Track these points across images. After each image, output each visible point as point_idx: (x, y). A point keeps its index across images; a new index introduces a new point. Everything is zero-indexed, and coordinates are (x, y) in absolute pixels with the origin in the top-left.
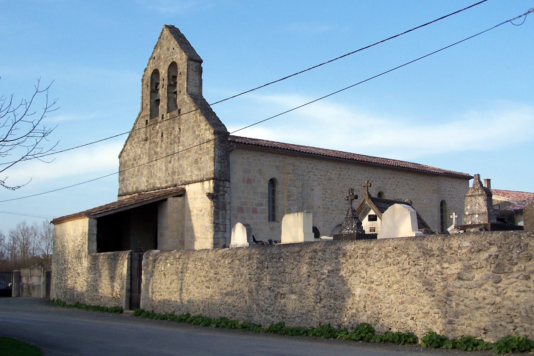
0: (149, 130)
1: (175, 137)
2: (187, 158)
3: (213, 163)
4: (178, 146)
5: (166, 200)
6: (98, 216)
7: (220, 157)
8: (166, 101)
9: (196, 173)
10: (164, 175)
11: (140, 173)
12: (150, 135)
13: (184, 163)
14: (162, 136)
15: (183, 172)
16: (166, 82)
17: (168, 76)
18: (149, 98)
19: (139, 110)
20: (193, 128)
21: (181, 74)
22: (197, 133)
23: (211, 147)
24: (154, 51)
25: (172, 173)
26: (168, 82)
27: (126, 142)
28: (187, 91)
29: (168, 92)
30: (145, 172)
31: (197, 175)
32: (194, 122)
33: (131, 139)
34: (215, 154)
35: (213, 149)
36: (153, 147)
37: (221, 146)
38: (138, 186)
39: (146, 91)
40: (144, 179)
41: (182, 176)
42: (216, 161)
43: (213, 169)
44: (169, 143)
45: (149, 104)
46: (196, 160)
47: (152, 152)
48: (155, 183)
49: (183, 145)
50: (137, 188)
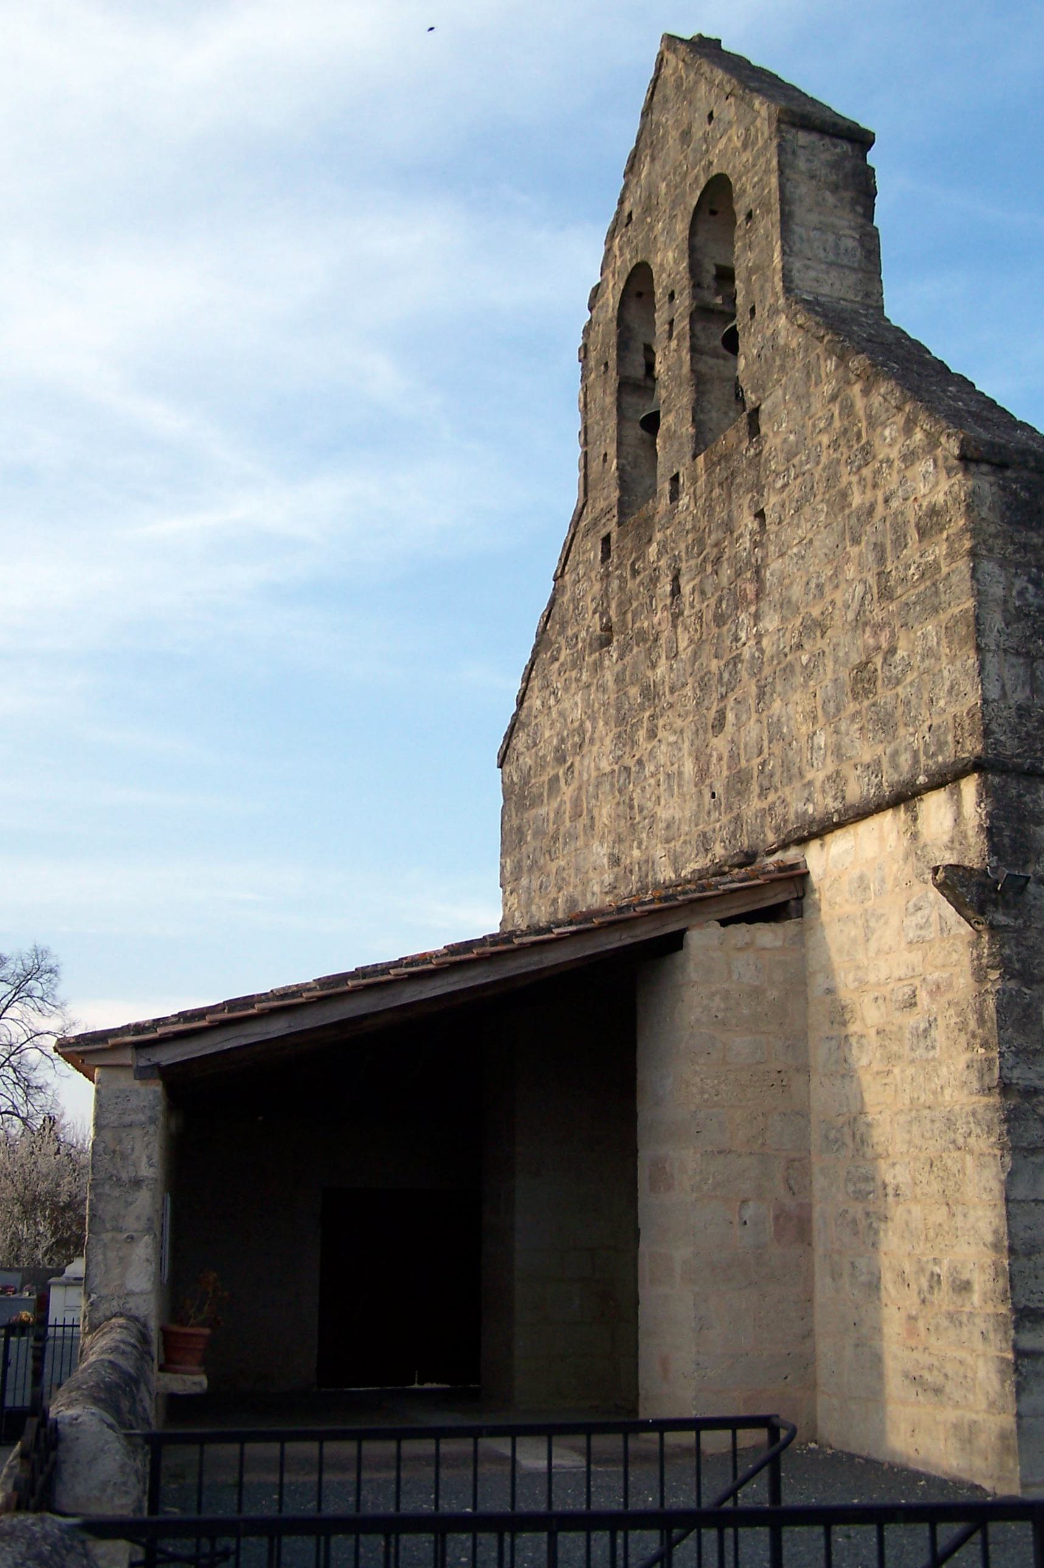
0: (615, 584)
1: (738, 574)
2: (809, 672)
3: (972, 661)
4: (757, 617)
5: (675, 942)
6: (167, 1056)
7: (1016, 616)
8: (685, 399)
9: (867, 758)
10: (691, 806)
11: (584, 819)
12: (620, 604)
13: (792, 707)
14: (676, 591)
15: (786, 766)
16: (684, 302)
17: (694, 268)
18: (612, 423)
19: (571, 498)
20: (832, 478)
21: (749, 216)
22: (857, 499)
23: (952, 556)
24: (626, 187)
25: (728, 788)
26: (694, 297)
27: (527, 679)
28: (788, 290)
29: (694, 349)
30: (605, 812)
31: (874, 767)
32: (835, 445)
33: (545, 656)
34: (979, 595)
35: (963, 565)
36: (635, 666)
37: (1024, 547)
38: (577, 895)
39: (599, 392)
40: (600, 851)
41: (787, 792)
42: (990, 640)
43: (973, 699)
44: (708, 616)
45: (612, 451)
46: (862, 667)
47: (634, 691)
48: (649, 862)
49: (786, 605)
50: (572, 902)
